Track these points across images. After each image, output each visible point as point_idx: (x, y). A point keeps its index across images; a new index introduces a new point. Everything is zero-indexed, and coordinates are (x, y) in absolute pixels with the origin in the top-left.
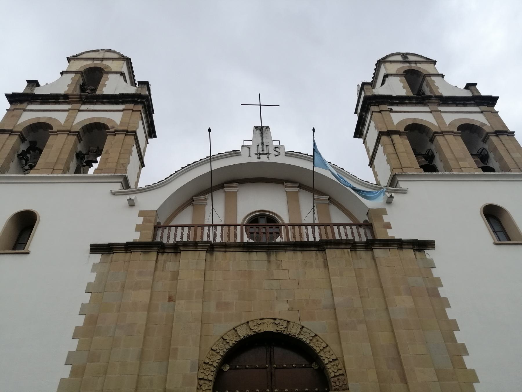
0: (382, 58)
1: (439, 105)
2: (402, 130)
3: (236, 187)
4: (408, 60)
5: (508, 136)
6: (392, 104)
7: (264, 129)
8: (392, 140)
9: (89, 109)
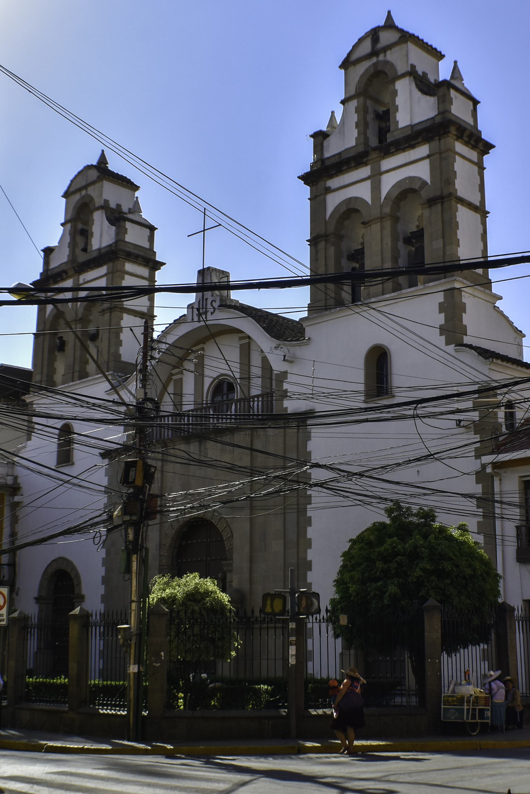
0: (345, 55)
1: (383, 158)
2: (331, 229)
3: (203, 349)
4: (380, 46)
5: (442, 203)
6: (331, 177)
7: (205, 272)
8: (317, 252)
9: (86, 280)
